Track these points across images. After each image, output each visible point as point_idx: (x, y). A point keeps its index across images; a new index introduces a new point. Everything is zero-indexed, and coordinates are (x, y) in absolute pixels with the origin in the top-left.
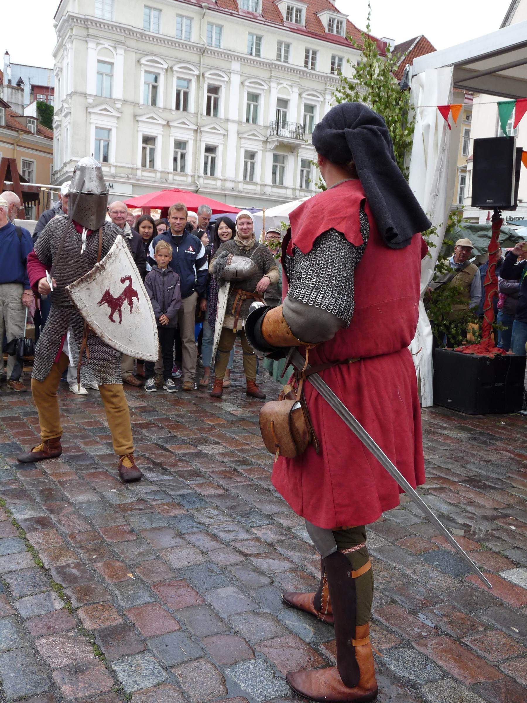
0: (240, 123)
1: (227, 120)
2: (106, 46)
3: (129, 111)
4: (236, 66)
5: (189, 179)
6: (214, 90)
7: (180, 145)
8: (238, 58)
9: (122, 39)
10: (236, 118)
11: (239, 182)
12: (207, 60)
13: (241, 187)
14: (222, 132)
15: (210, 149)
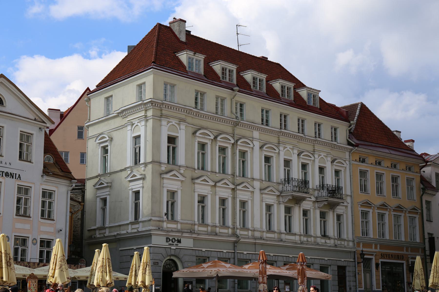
0: (261, 180)
1: (253, 179)
2: (174, 123)
3: (189, 174)
4: (256, 134)
5: (230, 231)
6: (243, 154)
7: (223, 201)
8: (258, 129)
9: (183, 117)
10: (258, 178)
11: (263, 232)
12: (239, 131)
13: (265, 235)
14: (251, 189)
15: (243, 204)
